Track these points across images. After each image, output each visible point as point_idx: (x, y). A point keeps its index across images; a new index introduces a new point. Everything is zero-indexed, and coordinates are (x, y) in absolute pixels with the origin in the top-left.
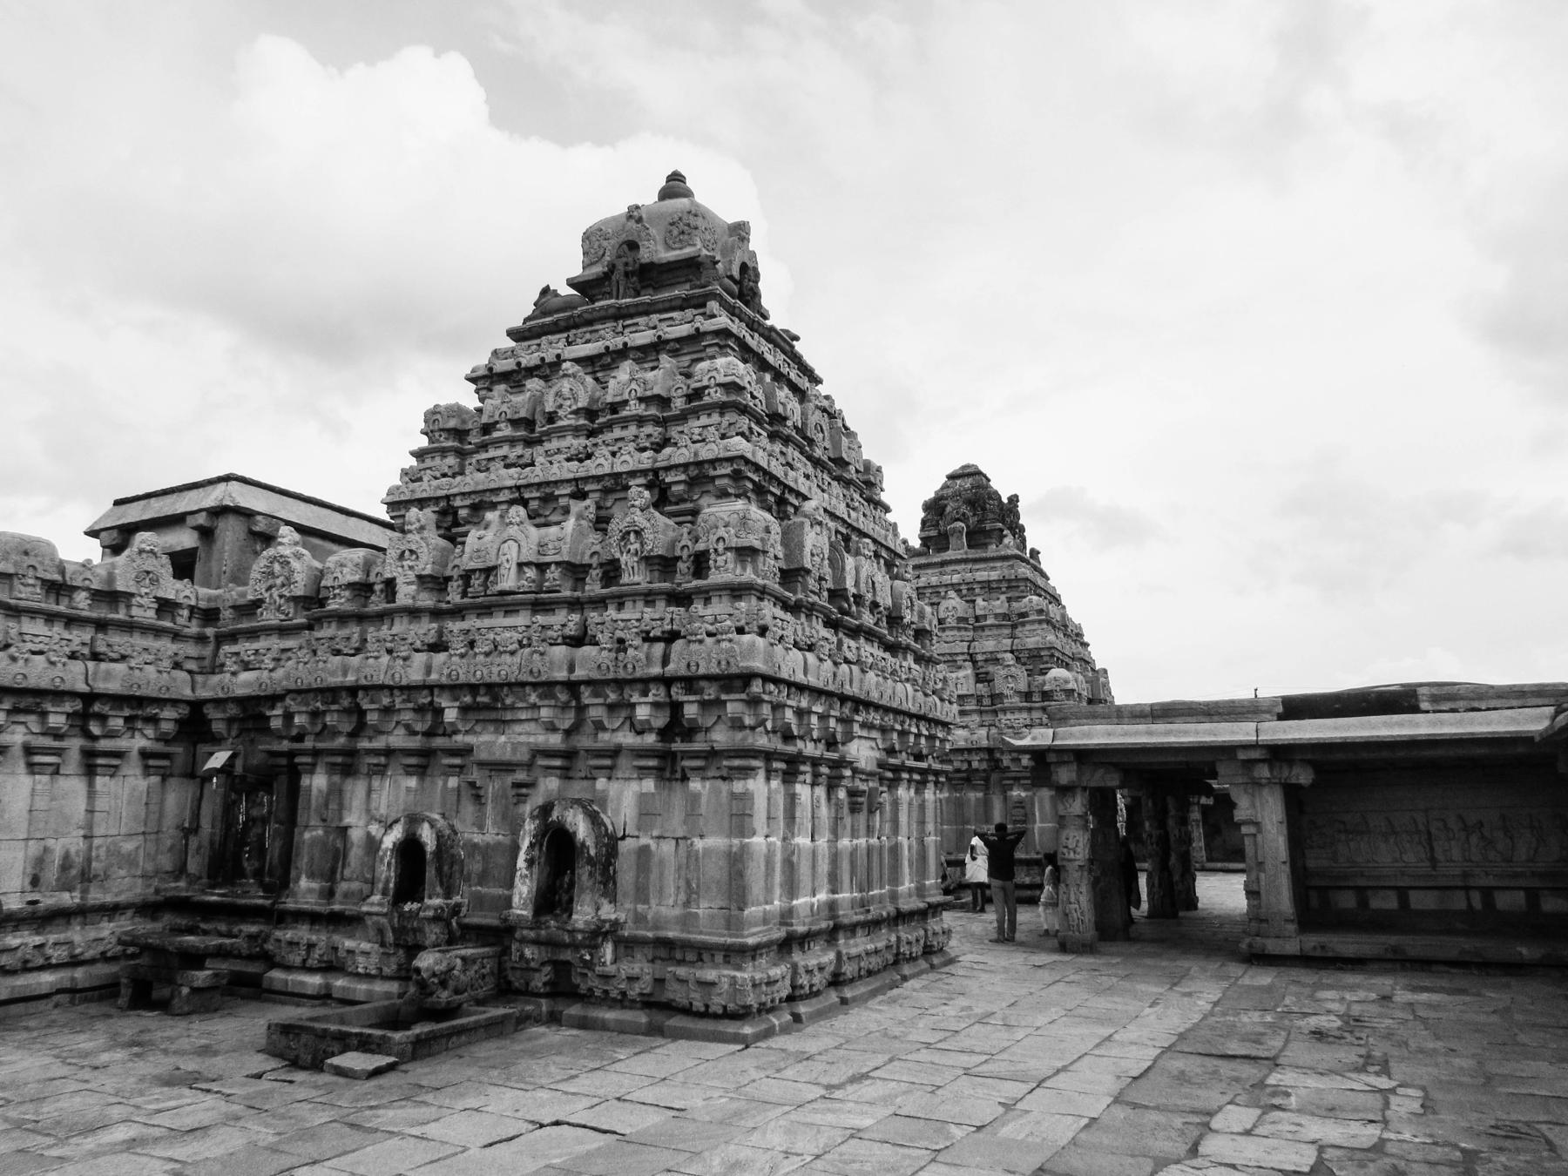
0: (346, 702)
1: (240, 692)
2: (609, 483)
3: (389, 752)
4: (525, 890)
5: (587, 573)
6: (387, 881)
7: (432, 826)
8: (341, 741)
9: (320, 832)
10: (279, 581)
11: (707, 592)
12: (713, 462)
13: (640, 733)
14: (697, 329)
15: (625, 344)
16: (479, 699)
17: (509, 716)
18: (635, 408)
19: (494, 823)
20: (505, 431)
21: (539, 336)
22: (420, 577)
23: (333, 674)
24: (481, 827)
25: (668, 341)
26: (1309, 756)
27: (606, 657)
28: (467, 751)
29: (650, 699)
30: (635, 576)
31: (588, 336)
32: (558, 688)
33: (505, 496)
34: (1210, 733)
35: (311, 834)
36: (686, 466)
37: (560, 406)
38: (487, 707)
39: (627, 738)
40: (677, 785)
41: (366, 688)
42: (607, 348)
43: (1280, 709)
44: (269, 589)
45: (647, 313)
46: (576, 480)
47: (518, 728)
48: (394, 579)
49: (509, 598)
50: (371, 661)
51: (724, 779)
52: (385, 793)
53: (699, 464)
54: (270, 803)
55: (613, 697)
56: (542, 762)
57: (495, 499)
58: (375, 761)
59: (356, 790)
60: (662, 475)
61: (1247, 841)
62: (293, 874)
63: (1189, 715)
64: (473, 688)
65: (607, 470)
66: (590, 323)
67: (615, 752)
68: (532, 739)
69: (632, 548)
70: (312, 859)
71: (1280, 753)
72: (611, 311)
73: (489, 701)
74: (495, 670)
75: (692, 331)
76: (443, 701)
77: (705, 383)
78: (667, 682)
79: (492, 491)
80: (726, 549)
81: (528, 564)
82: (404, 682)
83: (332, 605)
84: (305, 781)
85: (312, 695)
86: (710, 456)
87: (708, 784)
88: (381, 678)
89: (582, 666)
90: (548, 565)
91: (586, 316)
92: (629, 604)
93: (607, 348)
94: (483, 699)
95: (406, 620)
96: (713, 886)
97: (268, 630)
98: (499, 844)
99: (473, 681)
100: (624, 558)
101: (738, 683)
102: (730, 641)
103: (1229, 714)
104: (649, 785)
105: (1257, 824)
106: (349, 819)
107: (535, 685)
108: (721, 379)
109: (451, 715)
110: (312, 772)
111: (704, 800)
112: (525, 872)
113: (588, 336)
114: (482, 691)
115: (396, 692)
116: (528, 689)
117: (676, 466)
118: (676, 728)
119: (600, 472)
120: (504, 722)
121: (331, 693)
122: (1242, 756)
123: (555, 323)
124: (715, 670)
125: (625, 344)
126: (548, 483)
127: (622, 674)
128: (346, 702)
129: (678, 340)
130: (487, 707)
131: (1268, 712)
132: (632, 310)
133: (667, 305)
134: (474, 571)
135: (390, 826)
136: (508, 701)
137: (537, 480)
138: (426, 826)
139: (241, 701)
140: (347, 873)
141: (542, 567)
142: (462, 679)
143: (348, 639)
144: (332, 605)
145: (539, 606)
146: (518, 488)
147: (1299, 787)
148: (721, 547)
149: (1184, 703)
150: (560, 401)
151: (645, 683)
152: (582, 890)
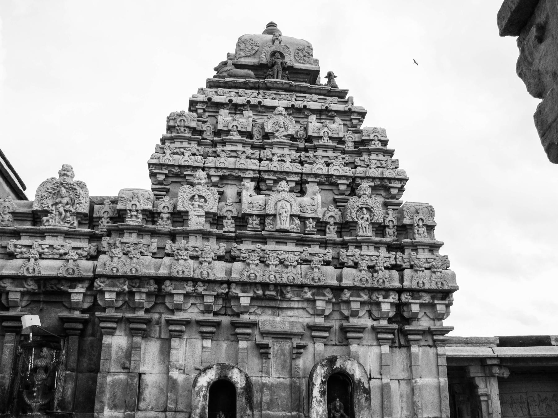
0: (153, 287)
1: (45, 273)
2: (323, 179)
3: (187, 323)
4: (320, 410)
5: (325, 227)
6: (204, 408)
7: (241, 372)
8: (141, 314)
9: (122, 377)
10: (65, 200)
11: (416, 246)
12: (390, 179)
13: (375, 320)
14: (350, 109)
15: (305, 106)
16: (268, 293)
17: (285, 305)
18: (326, 141)
19: (277, 371)
20: (237, 137)
21: (230, 87)
22: (207, 213)
23: (147, 267)
24: (268, 374)
25: (331, 111)
26: (509, 364)
27: (365, 274)
28: (253, 325)
29: (391, 300)
30: (365, 231)
31: (274, 96)
32: (328, 290)
33: (251, 174)
34: (483, 352)
35: (113, 377)
36: (374, 179)
37: (277, 131)
38: (272, 299)
39: (365, 321)
40: (397, 349)
41: (171, 279)
42: (293, 106)
43: (498, 342)
44: (56, 204)
45: (311, 94)
46: (302, 174)
47: (290, 313)
48: (187, 212)
49: (285, 234)
50: (181, 262)
51: (430, 346)
52: (182, 351)
53: (382, 179)
54: (58, 356)
55: (365, 297)
56: (362, 330)
57: (242, 175)
58: (178, 328)
59: (151, 350)
60: (358, 181)
61: (483, 405)
62: (97, 406)
63: (459, 343)
64: (265, 286)
65: (325, 172)
66: (269, 89)
67: (361, 329)
68: (300, 320)
69: (365, 218)
70: (114, 396)
71: (503, 361)
72: (286, 86)
73: (272, 295)
74: (285, 276)
75: (347, 109)
76: (236, 291)
77: (372, 137)
78: (400, 291)
79: (240, 170)
80: (424, 225)
81: (295, 216)
82: (211, 277)
83: (131, 222)
84: (107, 340)
85: (122, 280)
86: (391, 176)
87: (421, 349)
88: (189, 274)
89: (347, 279)
90: (309, 218)
91: (268, 84)
92: (364, 247)
93: (293, 106)
94: (272, 293)
95: (200, 239)
96: (429, 405)
97: (132, 229)
98: (281, 383)
99: (268, 281)
100: (360, 222)
101: (440, 295)
102: (441, 272)
103: (476, 343)
104: (386, 349)
105: (487, 395)
106: (142, 369)
107: (310, 287)
108: (380, 138)
109: (245, 301)
110: (112, 334)
111: (420, 357)
112: (319, 398)
113: (274, 96)
114: (272, 288)
115: (200, 284)
116: (306, 289)
117: (368, 178)
118: (401, 316)
119: (320, 172)
120: (279, 308)
121: (137, 280)
122: (489, 362)
123: (245, 83)
124: (434, 287)
125: (305, 106)
126: (281, 172)
127: (376, 285)
128: (153, 287)
129: (336, 112)
130: (272, 299)
131: (493, 343)
132: (297, 89)
133: (318, 91)
134: (251, 215)
135: (205, 371)
136: (289, 296)
137: (275, 169)
138: (236, 371)
139: (40, 280)
140: (142, 405)
141: (303, 220)
142: (259, 279)
143: (149, 245)
144: (131, 222)
145: (301, 242)
146: (260, 171)
147: (503, 378)
148: (421, 223)
149: (454, 337)
150: (277, 128)
151: (387, 291)
152: (361, 408)
